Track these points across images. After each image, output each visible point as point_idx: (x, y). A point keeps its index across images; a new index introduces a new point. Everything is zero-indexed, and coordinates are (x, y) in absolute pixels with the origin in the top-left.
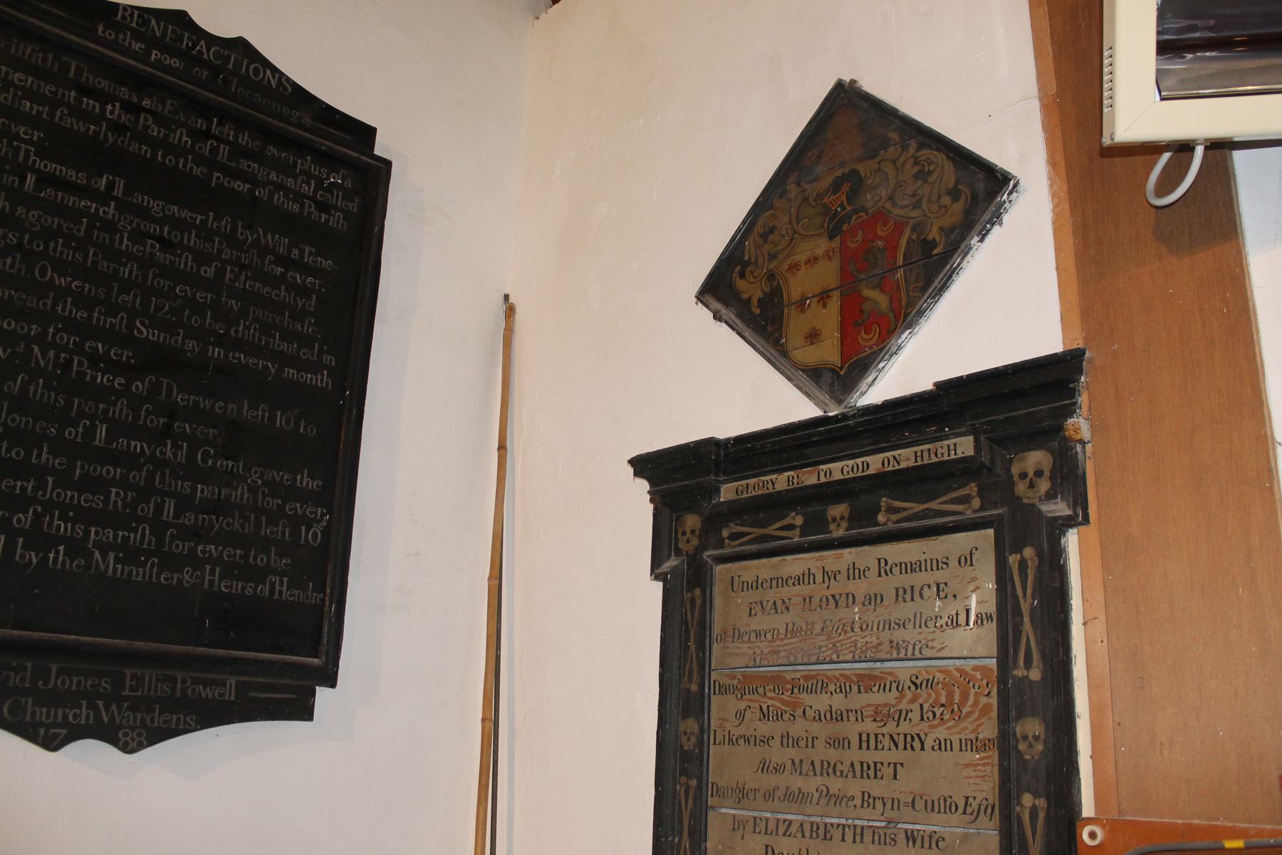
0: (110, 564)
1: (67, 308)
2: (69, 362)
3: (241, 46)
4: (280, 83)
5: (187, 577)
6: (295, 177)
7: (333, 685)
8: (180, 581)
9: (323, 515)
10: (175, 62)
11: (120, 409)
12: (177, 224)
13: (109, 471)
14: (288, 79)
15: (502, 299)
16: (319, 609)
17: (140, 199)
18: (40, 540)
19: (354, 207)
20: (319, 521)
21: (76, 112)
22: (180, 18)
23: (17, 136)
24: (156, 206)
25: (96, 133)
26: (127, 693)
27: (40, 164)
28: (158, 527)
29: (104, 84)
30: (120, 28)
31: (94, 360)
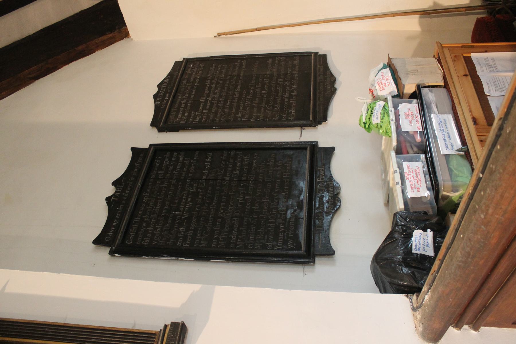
0: (294, 87)
1: (236, 101)
2: (248, 99)
3: (159, 86)
4: (168, 78)
5: (296, 75)
6: (192, 73)
7: (318, 52)
8: (297, 76)
9: (278, 58)
10: (167, 95)
11: (258, 90)
12: (210, 88)
13: (273, 89)
14: (166, 77)
15: (216, 38)
16: (300, 56)
17: (205, 94)
18: (291, 96)
19: (198, 63)
20: (279, 58)
21: (186, 107)
22: (155, 97)
23: (195, 115)
24: (206, 92)
25: (190, 104)
26: (323, 81)
27: (201, 110)
28: (285, 81)
29: (177, 105)
30: (161, 105)
31: (246, 95)
